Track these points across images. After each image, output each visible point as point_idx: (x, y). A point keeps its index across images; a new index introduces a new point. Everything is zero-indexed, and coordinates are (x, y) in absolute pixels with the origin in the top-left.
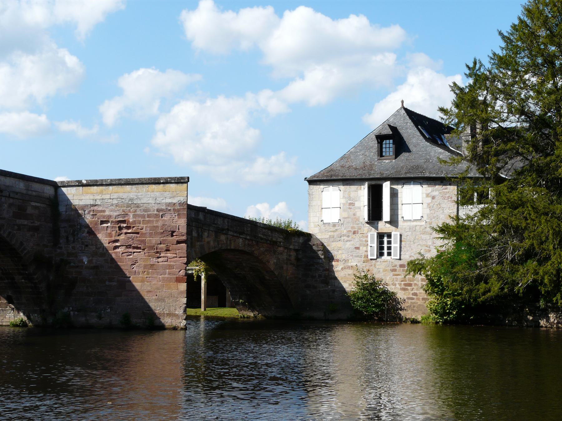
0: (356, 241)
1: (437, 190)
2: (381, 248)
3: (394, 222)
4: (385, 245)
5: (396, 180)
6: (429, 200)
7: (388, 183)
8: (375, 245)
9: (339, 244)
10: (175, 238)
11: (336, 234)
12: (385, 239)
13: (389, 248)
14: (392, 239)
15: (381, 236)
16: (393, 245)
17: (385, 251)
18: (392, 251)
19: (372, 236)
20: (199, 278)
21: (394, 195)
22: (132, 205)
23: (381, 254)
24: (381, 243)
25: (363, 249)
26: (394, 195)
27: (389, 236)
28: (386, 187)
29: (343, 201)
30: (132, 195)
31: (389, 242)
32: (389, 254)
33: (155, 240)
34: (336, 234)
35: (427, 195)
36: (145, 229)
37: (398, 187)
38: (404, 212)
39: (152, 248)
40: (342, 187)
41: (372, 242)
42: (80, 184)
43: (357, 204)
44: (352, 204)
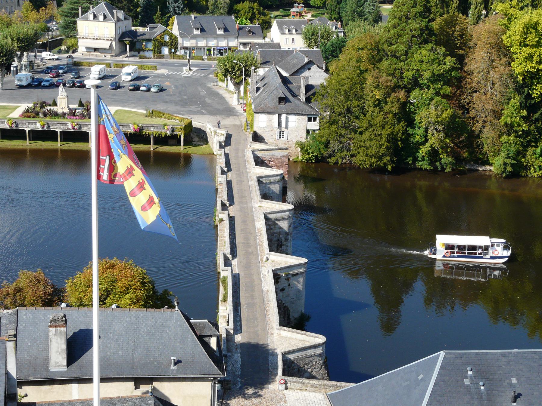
0: (272, 133)
1: (301, 117)
2: (280, 136)
3: (287, 127)
4: (282, 135)
5: (288, 114)
6: (298, 120)
7: (285, 115)
8: (279, 135)
9: (265, 134)
10: (285, 164)
11: (264, 131)
12: (282, 133)
13: (283, 136)
14: (284, 133)
15: (280, 132)
16: (284, 135)
17: (282, 136)
18: (284, 137)
19: (278, 132)
20: (180, 136)
21: (287, 118)
22: (273, 155)
23: (280, 138)
24: (280, 134)
25: (274, 136)
26: (287, 118)
27: (283, 132)
28: (283, 117)
29: (267, 120)
30: (273, 153)
31: (283, 134)
32: (283, 137)
33: (279, 165)
34: (264, 131)
35: (297, 119)
36: (276, 162)
37: (288, 116)
38: (290, 124)
39: (278, 167)
40: (267, 115)
41: (278, 134)
42: (258, 150)
43: (272, 121)
44: (271, 121)
